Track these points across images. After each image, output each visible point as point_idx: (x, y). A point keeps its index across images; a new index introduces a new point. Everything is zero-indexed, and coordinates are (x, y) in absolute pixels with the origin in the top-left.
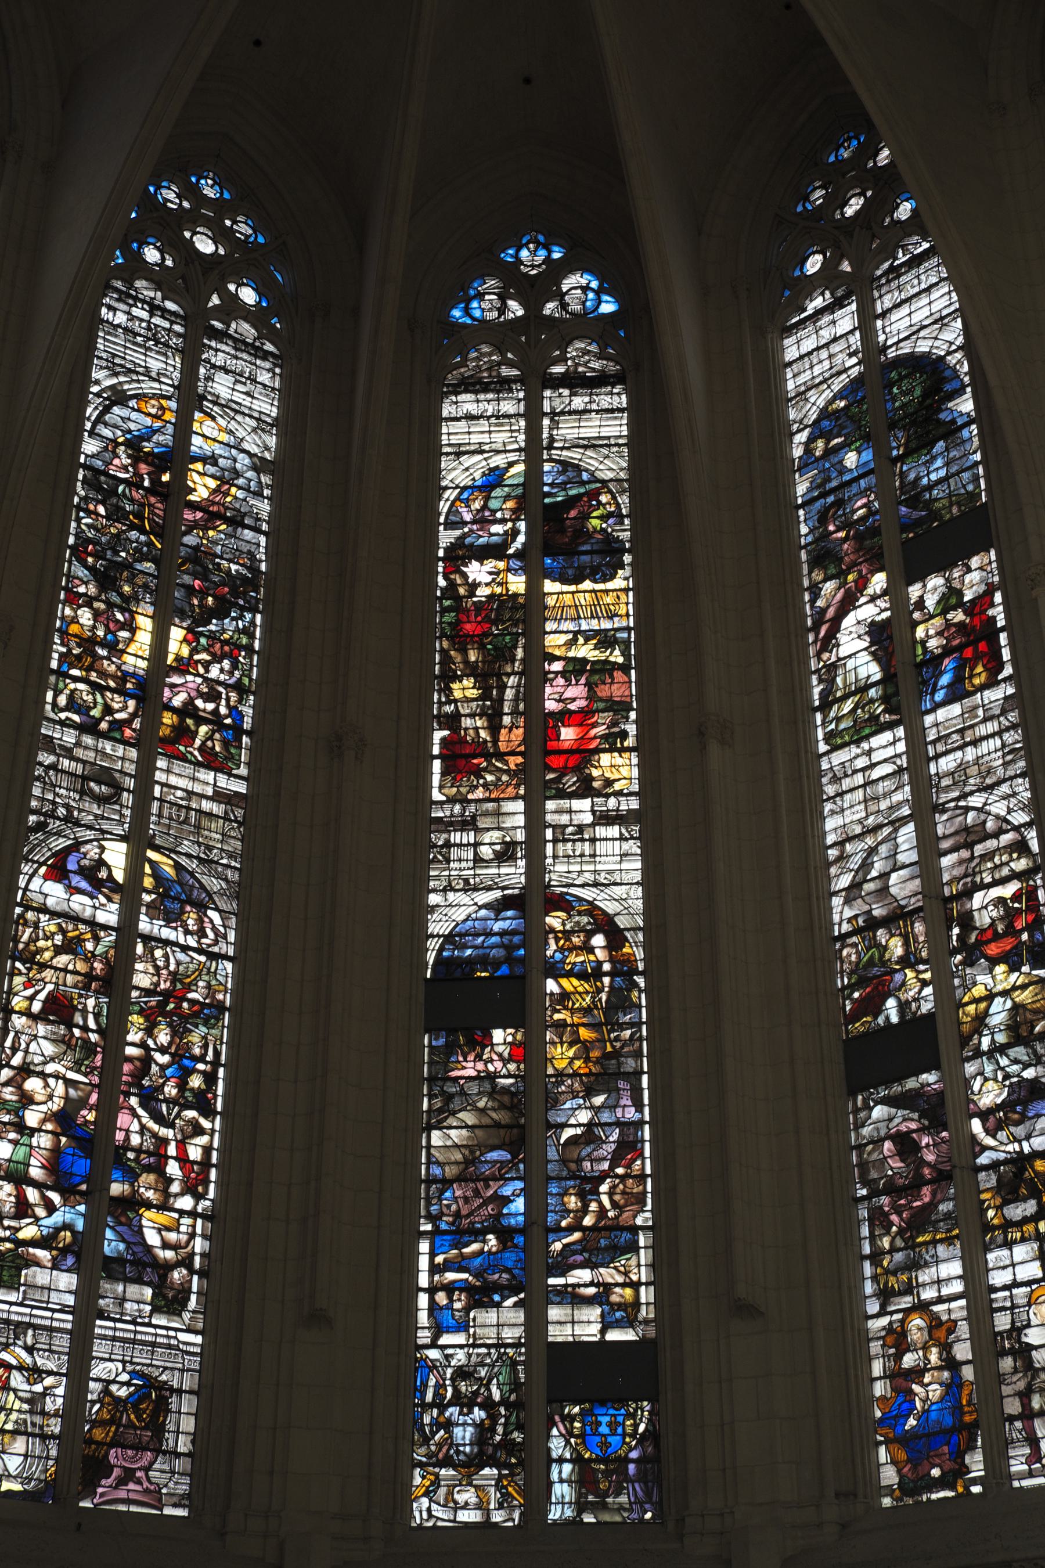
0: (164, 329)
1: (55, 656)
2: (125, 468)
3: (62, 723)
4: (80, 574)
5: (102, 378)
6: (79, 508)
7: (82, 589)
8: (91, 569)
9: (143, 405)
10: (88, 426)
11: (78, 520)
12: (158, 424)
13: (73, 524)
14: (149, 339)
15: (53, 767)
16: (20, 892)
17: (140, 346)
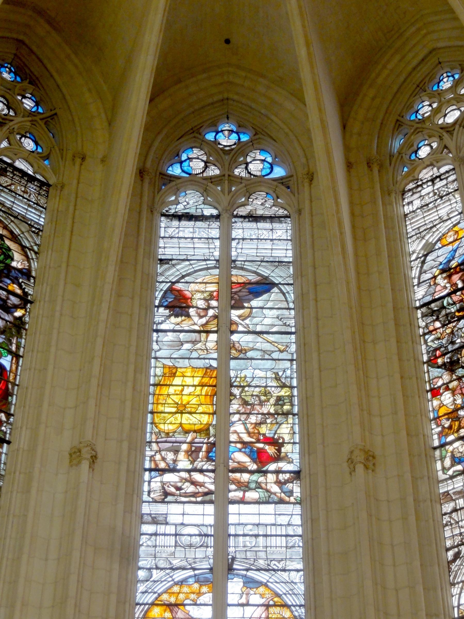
0: (443, 186)
1: (436, 437)
2: (445, 287)
3: (452, 477)
4: (436, 374)
5: (415, 246)
6: (425, 334)
7: (440, 383)
8: (444, 366)
9: (444, 242)
10: (416, 282)
11: (426, 342)
12: (456, 244)
13: (424, 347)
14: (436, 200)
15: (455, 510)
16: (456, 609)
17: (432, 209)
